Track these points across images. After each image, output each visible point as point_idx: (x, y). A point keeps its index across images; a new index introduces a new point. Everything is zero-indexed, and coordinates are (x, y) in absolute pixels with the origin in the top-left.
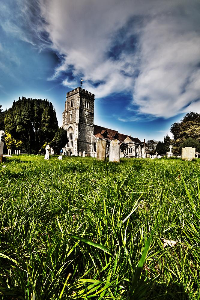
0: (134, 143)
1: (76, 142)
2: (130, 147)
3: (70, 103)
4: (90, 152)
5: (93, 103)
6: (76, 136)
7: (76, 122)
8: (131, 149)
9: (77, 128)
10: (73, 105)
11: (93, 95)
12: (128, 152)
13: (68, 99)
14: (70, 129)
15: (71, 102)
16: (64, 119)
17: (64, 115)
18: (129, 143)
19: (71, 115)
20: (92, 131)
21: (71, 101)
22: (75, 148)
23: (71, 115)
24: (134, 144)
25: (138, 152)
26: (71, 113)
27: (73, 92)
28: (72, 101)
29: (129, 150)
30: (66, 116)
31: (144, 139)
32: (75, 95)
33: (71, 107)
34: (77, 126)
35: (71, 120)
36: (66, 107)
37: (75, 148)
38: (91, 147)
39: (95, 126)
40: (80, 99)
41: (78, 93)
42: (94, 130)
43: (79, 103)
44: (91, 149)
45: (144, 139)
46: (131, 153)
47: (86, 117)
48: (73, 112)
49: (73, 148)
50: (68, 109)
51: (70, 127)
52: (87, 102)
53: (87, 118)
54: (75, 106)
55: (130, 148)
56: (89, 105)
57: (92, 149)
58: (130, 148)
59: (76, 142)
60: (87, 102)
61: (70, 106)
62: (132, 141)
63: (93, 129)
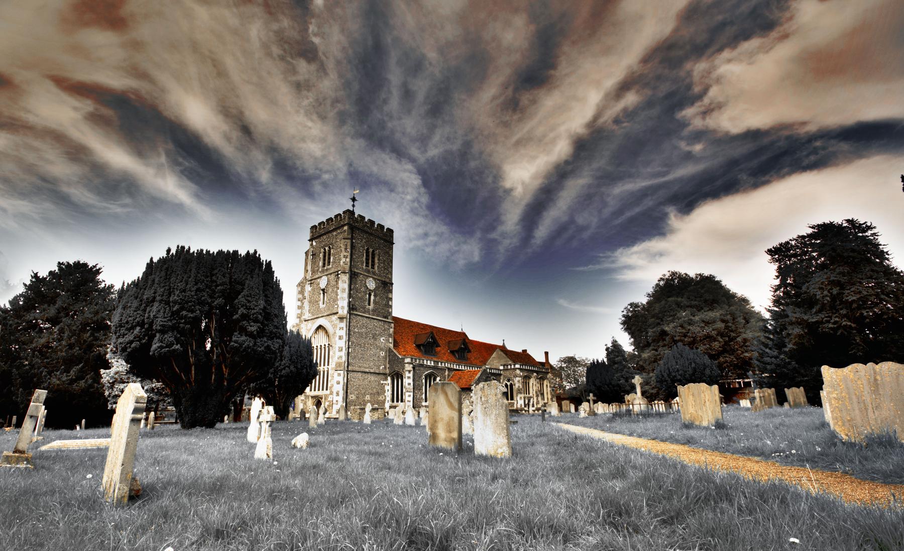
0: (517, 366)
1: (339, 375)
2: (509, 381)
3: (321, 255)
4: (384, 402)
5: (388, 253)
6: (338, 355)
7: (340, 312)
8: (511, 385)
10: (329, 262)
13: (314, 243)
14: (321, 333)
15: (325, 253)
16: (299, 303)
18: (501, 368)
21: (322, 250)
22: (338, 394)
23: (323, 290)
24: (518, 372)
25: (531, 395)
26: (323, 286)
30: (306, 294)
31: (546, 353)
33: (324, 265)
34: (343, 325)
35: (321, 306)
36: (309, 268)
37: (335, 394)
38: (388, 388)
39: (397, 320)
40: (352, 243)
41: (346, 228)
42: (395, 332)
43: (349, 254)
44: (388, 394)
45: (546, 353)
46: (512, 399)
47: (370, 295)
48: (328, 281)
49: (328, 392)
50: (313, 272)
52: (371, 250)
53: (372, 297)
54: (334, 262)
56: (379, 260)
57: (390, 392)
59: (339, 375)
60: (371, 250)
61: (321, 264)
63: (392, 330)
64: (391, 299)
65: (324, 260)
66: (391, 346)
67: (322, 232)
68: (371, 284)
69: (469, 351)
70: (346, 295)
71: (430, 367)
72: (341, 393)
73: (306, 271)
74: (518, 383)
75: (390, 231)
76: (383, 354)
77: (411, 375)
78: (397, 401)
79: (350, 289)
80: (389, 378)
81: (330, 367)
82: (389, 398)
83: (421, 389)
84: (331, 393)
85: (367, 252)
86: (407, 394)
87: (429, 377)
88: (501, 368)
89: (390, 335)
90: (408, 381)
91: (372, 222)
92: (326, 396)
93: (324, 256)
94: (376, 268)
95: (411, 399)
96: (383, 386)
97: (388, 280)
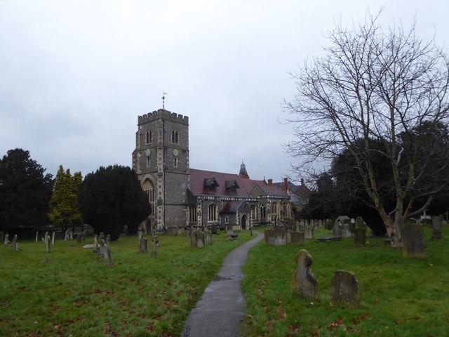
8: (264, 209)
9: (160, 181)
11: (186, 118)
12: (260, 216)
24: (269, 200)
29: (259, 212)
30: (138, 159)
36: (139, 143)
41: (160, 120)
44: (188, 217)
46: (265, 217)
50: (141, 144)
51: (147, 179)
64: (188, 160)
67: (146, 121)
68: (176, 152)
69: (238, 187)
70: (161, 162)
71: (211, 201)
72: (162, 217)
73: (137, 145)
74: (268, 207)
75: (186, 118)
76: (184, 194)
77: (200, 206)
79: (164, 158)
84: (156, 217)
85: (173, 133)
87: (211, 206)
90: (199, 209)
91: (175, 114)
92: (153, 219)
95: (200, 220)
96: (185, 212)
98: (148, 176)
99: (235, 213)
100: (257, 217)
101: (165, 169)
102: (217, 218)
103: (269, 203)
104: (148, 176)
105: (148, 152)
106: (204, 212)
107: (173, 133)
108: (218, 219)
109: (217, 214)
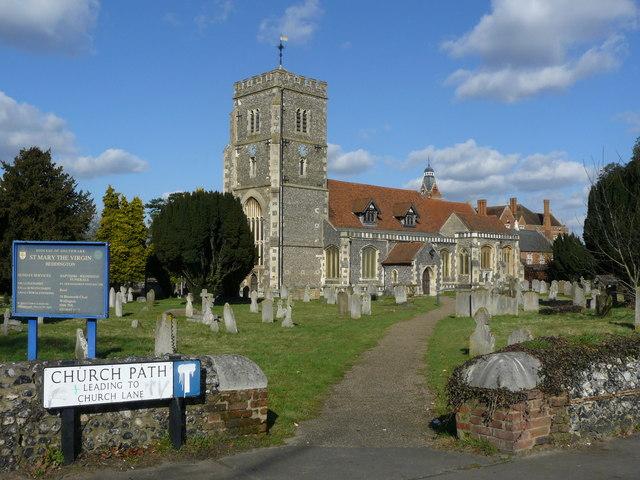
0: (475, 235)
1: (274, 251)
3: (249, 118)
9: (275, 204)
13: (240, 104)
15: (253, 116)
16: (226, 171)
17: (229, 159)
19: (253, 158)
20: (325, 205)
21: (249, 113)
24: (475, 241)
26: (252, 152)
27: (254, 83)
28: (255, 111)
30: (234, 161)
32: (262, 95)
41: (275, 90)
44: (324, 268)
45: (546, 203)
46: (467, 272)
47: (302, 162)
50: (240, 136)
52: (302, 111)
54: (263, 129)
55: (464, 255)
57: (325, 268)
58: (464, 255)
60: (302, 111)
61: (249, 128)
62: (467, 230)
63: (327, 199)
65: (252, 124)
66: (327, 216)
70: (278, 168)
74: (476, 254)
77: (348, 250)
78: (334, 276)
79: (282, 159)
80: (324, 252)
81: (264, 242)
82: (324, 273)
83: (358, 264)
84: (267, 268)
86: (344, 269)
88: (457, 236)
89: (325, 205)
90: (344, 255)
93: (252, 119)
94: (308, 130)
95: (347, 274)
96: (317, 261)
97: (321, 143)
98: (252, 193)
99: (410, 265)
100: (453, 272)
101: (284, 180)
102: (377, 272)
103: (477, 247)
104: (252, 193)
105: (252, 150)
106: (354, 262)
107: (298, 114)
108: (380, 275)
109: (377, 264)
